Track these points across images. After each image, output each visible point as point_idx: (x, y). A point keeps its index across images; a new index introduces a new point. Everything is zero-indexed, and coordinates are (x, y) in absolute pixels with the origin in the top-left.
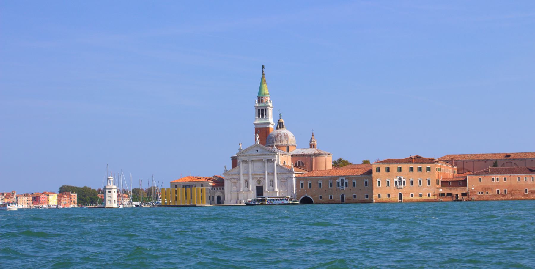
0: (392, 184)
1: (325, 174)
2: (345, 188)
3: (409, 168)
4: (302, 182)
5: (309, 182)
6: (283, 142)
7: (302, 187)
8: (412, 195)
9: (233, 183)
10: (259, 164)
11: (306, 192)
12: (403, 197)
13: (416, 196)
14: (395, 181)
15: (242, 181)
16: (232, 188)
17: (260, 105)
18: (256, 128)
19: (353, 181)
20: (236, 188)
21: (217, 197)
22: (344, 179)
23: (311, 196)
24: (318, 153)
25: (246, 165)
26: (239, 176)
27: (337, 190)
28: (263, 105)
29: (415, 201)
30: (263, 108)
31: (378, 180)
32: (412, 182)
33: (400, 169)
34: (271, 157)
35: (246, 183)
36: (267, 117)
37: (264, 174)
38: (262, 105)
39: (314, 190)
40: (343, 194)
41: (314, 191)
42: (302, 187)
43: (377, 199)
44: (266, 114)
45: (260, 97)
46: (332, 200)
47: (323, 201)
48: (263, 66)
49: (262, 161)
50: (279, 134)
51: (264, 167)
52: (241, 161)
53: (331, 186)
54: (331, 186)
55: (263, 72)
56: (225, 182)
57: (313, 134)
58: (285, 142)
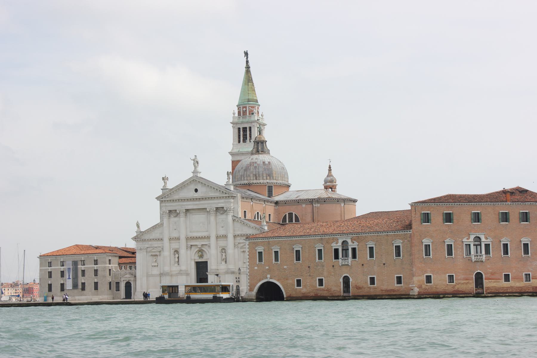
0: (459, 253)
1: (310, 230)
2: (350, 262)
3: (499, 213)
4: (260, 249)
5: (276, 248)
6: (261, 178)
7: (260, 260)
8: (507, 278)
11: (269, 271)
12: (484, 281)
13: (516, 278)
14: (465, 243)
17: (241, 120)
18: (232, 161)
19: (368, 246)
20: (158, 266)
22: (349, 241)
23: (278, 280)
24: (327, 196)
27: (333, 266)
28: (247, 119)
29: (514, 291)
31: (426, 241)
32: (506, 246)
33: (477, 218)
34: (222, 203)
37: (208, 238)
38: (244, 120)
39: (285, 267)
40: (346, 275)
42: (260, 260)
43: (424, 286)
44: (250, 137)
45: (241, 107)
46: (323, 290)
49: (203, 210)
50: (253, 163)
52: (166, 212)
53: (320, 258)
54: (320, 258)
55: (247, 62)
57: (330, 167)
58: (265, 178)
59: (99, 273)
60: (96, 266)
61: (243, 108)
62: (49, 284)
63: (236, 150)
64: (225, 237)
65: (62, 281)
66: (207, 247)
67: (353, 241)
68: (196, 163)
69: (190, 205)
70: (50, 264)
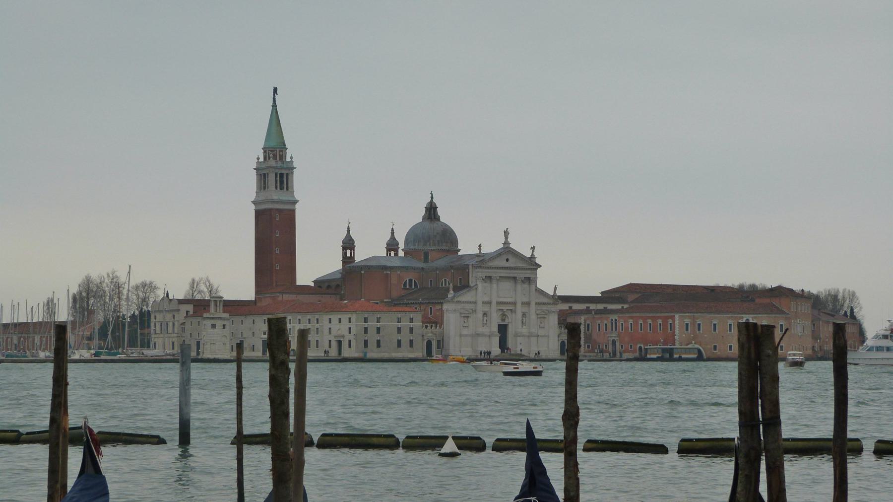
4: (687, 321)
5: (698, 322)
7: (687, 329)
9: (464, 317)
10: (507, 285)
11: (694, 338)
15: (480, 315)
16: (462, 327)
21: (427, 342)
26: (474, 305)
28: (284, 165)
30: (282, 172)
35: (485, 318)
36: (290, 190)
39: (706, 336)
42: (687, 329)
45: (278, 150)
47: (719, 353)
48: (275, 90)
51: (515, 290)
55: (274, 99)
61: (280, 151)
62: (365, 340)
63: (275, 197)
64: (528, 304)
66: (509, 311)
68: (506, 233)
69: (503, 273)
70: (366, 320)
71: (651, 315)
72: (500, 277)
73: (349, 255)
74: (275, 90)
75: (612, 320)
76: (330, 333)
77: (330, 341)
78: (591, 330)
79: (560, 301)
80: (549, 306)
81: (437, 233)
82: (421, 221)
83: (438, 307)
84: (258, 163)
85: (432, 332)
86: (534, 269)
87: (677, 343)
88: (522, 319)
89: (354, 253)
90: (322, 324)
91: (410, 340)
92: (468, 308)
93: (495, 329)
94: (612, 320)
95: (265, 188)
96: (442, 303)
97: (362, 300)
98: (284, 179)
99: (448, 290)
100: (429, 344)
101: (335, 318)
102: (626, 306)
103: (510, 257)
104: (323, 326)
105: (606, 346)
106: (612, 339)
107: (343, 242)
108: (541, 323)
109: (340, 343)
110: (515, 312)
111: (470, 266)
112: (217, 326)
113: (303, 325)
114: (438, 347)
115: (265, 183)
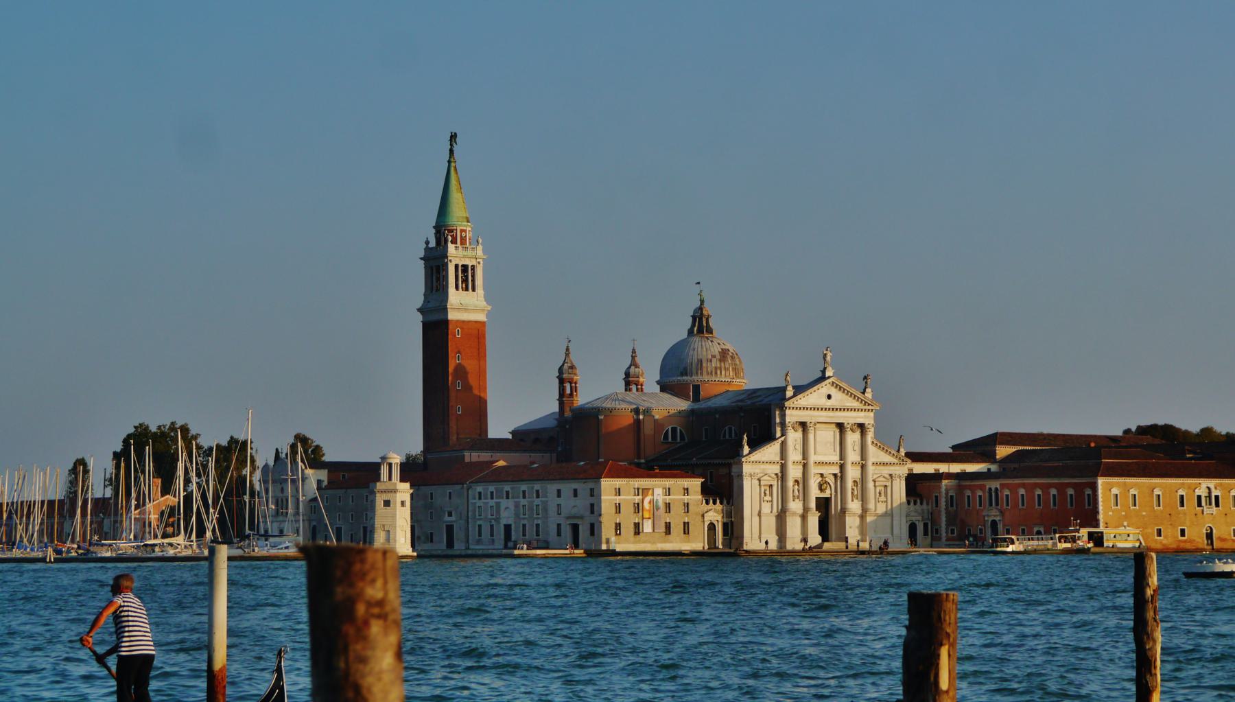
4: (1115, 491)
11: (1126, 517)
21: (709, 524)
22: (1212, 486)
25: (799, 434)
27: (1196, 515)
35: (796, 487)
39: (1144, 513)
40: (1210, 525)
41: (1144, 516)
44: (473, 281)
47: (1165, 542)
48: (453, 137)
54: (1182, 505)
55: (451, 151)
56: (744, 482)
57: (634, 351)
59: (691, 508)
60: (686, 497)
62: (616, 523)
65: (637, 519)
66: (832, 478)
67: (1218, 488)
70: (618, 492)
71: (1056, 481)
72: (818, 423)
73: (568, 391)
74: (453, 137)
75: (990, 489)
76: (559, 514)
77: (559, 525)
78: (956, 504)
79: (909, 461)
80: (892, 468)
81: (714, 356)
82: (684, 335)
83: (723, 471)
84: (427, 249)
85: (716, 511)
86: (869, 410)
87: (1102, 524)
88: (853, 489)
89: (576, 387)
90: (543, 499)
91: (684, 523)
92: (769, 471)
93: (813, 505)
94: (990, 489)
95: (437, 290)
96: (730, 466)
97: (600, 460)
98: (466, 276)
99: (741, 446)
100: (712, 527)
101: (567, 487)
102: (994, 468)
103: (833, 391)
104: (547, 501)
105: (981, 530)
106: (991, 519)
107: (561, 370)
108: (880, 493)
109: (575, 528)
110: (842, 477)
111: (773, 407)
112: (391, 503)
113: (513, 500)
114: (725, 533)
115: (438, 279)
